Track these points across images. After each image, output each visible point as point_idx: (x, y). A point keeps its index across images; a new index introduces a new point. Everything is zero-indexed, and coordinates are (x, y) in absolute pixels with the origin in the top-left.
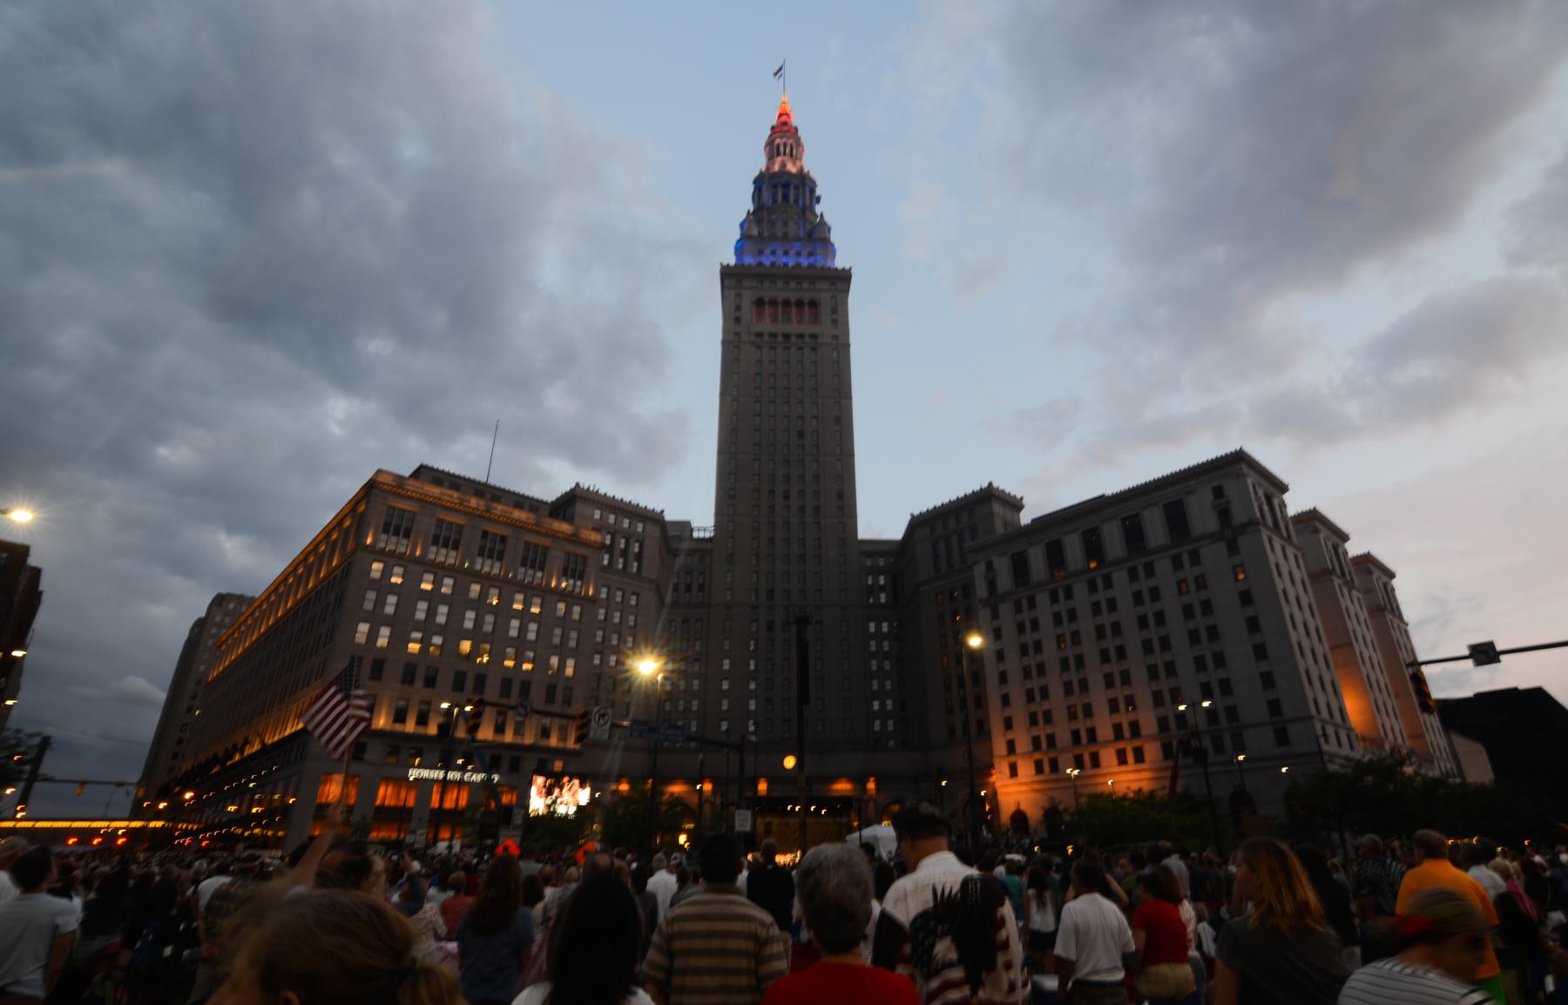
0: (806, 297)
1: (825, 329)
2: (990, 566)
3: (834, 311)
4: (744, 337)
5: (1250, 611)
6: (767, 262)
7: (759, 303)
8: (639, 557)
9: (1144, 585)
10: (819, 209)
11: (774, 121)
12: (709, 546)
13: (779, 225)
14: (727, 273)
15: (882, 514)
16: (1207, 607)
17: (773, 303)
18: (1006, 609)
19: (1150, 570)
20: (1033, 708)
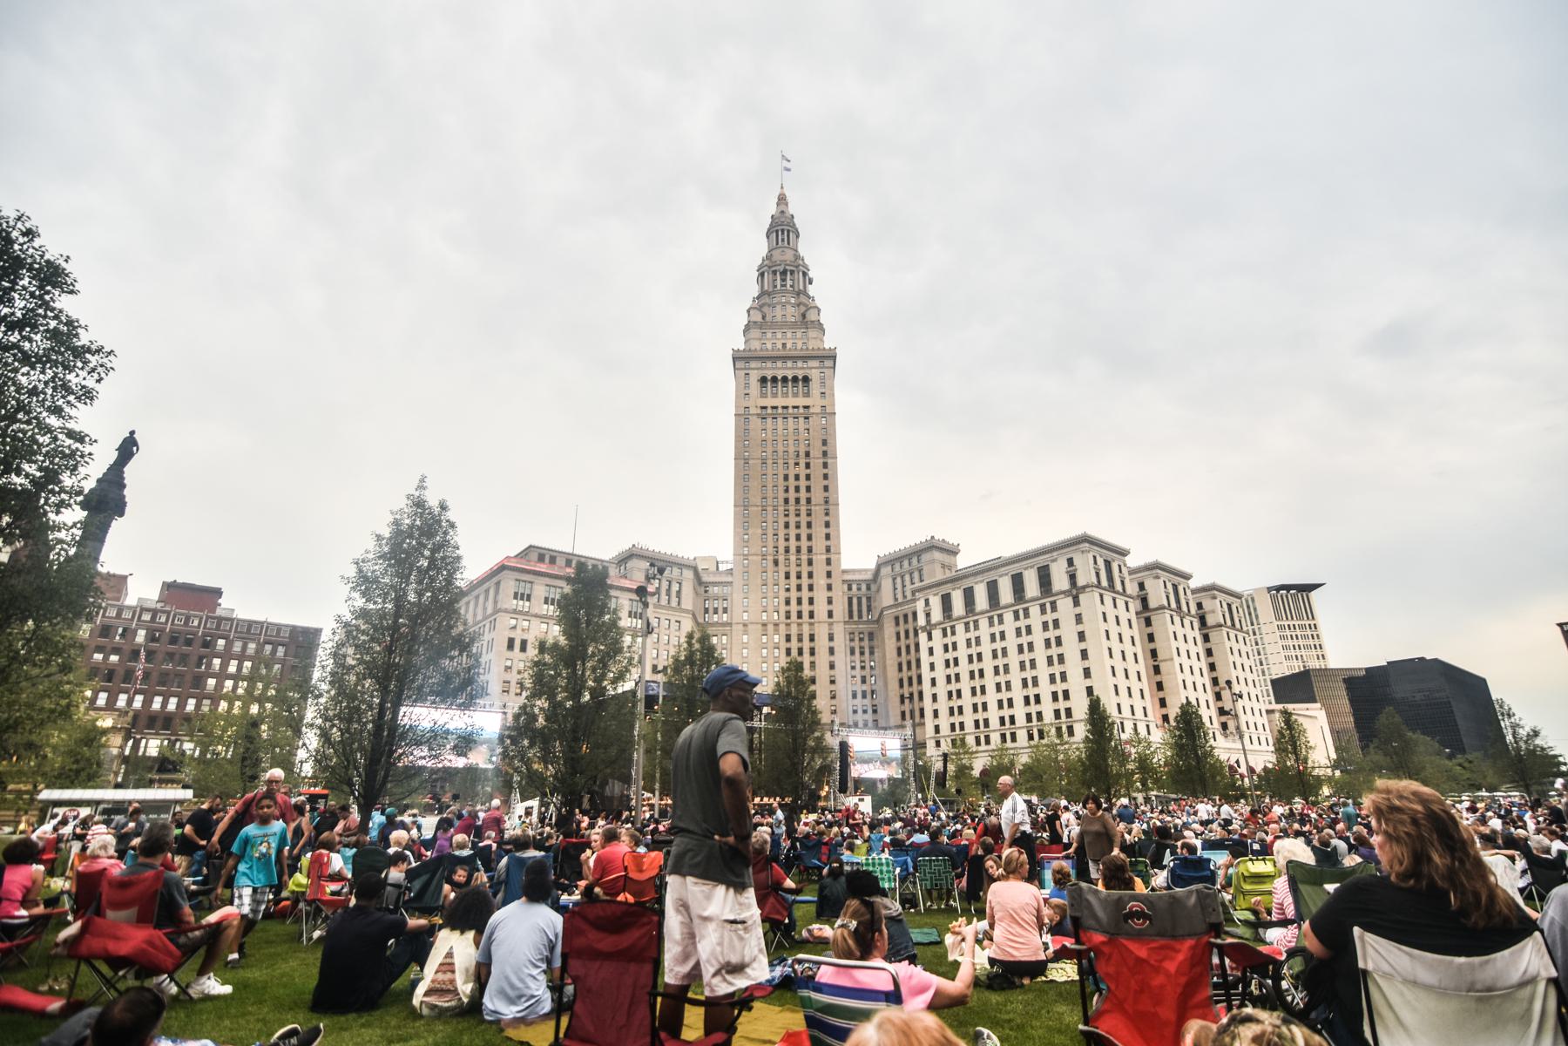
0: (800, 374)
1: (815, 401)
2: (927, 602)
3: (823, 383)
4: (753, 411)
5: (1083, 646)
6: (769, 346)
7: (763, 380)
8: (679, 593)
9: (1022, 623)
10: (811, 290)
11: (772, 209)
12: (729, 579)
13: (779, 307)
14: (738, 358)
15: (859, 549)
16: (1059, 641)
17: (774, 379)
18: (937, 633)
19: (1026, 611)
20: (952, 704)
